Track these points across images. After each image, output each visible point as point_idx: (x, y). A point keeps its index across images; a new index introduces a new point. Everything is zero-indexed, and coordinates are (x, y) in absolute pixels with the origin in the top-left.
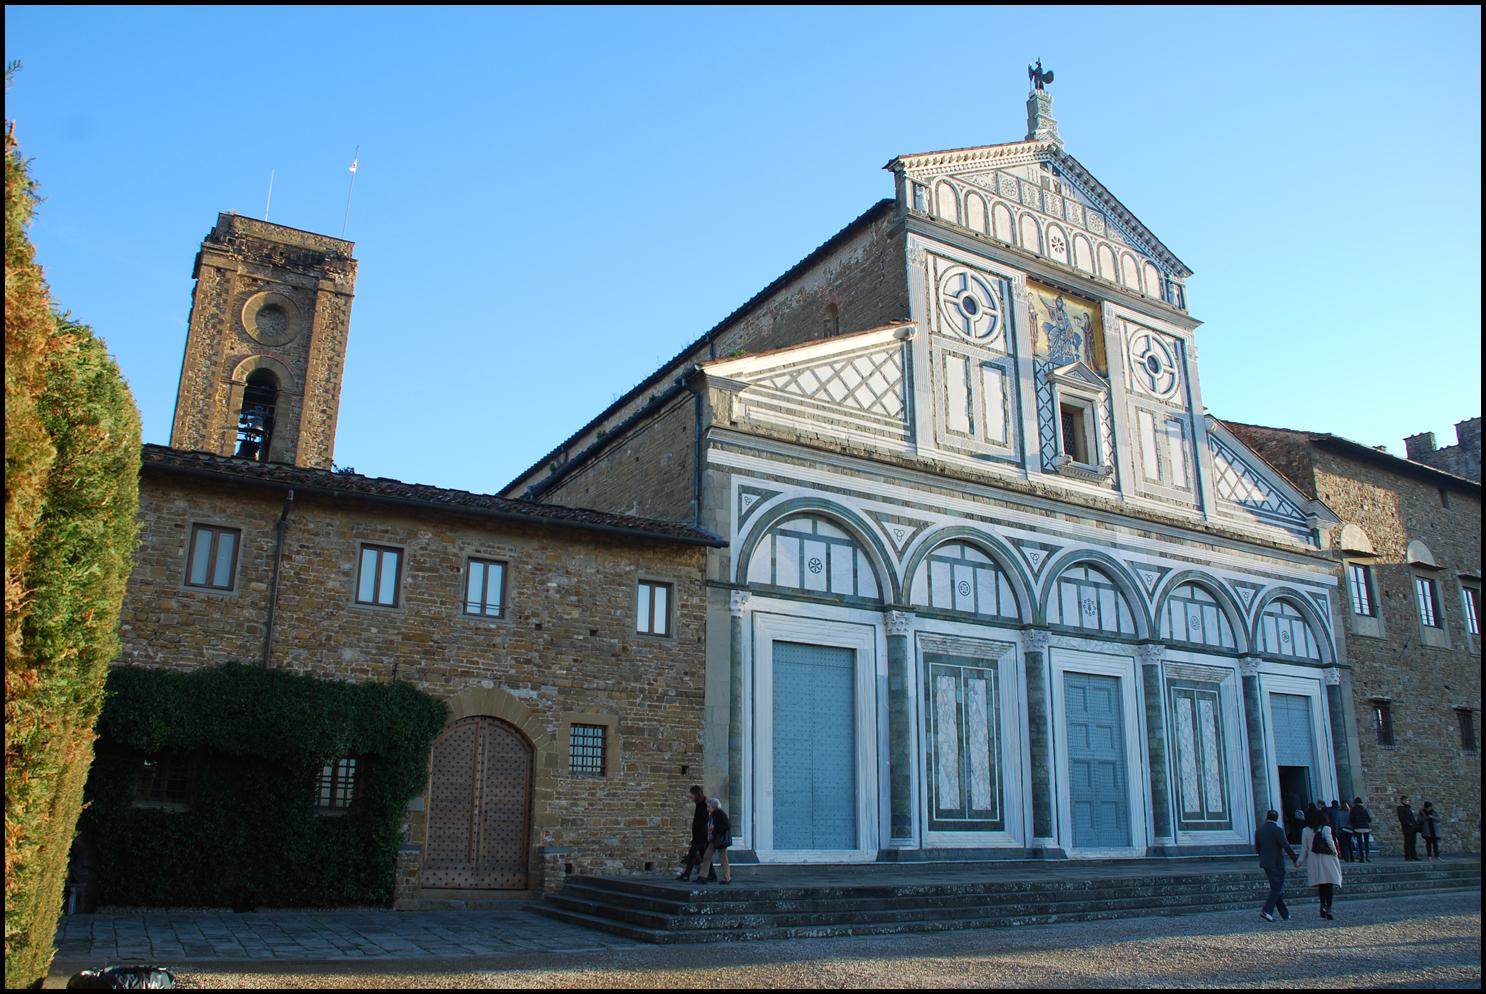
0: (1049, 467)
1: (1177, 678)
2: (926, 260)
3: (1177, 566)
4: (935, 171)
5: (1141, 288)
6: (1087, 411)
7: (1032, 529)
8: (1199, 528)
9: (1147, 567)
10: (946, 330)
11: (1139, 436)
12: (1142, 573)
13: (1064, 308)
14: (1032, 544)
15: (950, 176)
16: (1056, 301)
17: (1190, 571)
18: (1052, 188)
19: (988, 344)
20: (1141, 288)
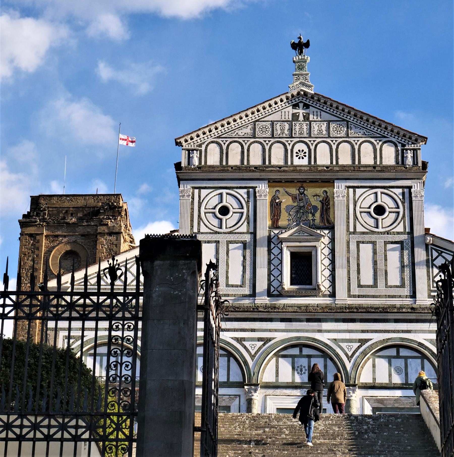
0: (276, 293)
1: (384, 407)
2: (193, 194)
3: (376, 337)
4: (206, 138)
5: (375, 162)
6: (313, 253)
7: (253, 330)
8: (404, 310)
9: (351, 341)
10: (203, 229)
11: (358, 259)
12: (344, 345)
13: (305, 192)
14: (252, 339)
15: (217, 137)
16: (299, 190)
17: (389, 339)
18: (301, 118)
19: (234, 230)
20: (375, 162)
